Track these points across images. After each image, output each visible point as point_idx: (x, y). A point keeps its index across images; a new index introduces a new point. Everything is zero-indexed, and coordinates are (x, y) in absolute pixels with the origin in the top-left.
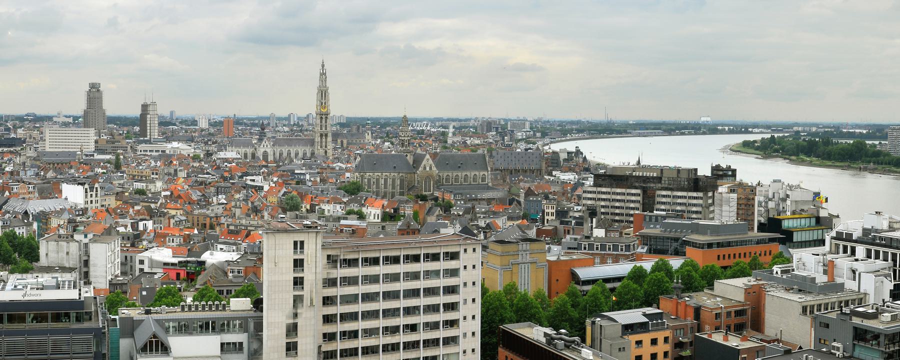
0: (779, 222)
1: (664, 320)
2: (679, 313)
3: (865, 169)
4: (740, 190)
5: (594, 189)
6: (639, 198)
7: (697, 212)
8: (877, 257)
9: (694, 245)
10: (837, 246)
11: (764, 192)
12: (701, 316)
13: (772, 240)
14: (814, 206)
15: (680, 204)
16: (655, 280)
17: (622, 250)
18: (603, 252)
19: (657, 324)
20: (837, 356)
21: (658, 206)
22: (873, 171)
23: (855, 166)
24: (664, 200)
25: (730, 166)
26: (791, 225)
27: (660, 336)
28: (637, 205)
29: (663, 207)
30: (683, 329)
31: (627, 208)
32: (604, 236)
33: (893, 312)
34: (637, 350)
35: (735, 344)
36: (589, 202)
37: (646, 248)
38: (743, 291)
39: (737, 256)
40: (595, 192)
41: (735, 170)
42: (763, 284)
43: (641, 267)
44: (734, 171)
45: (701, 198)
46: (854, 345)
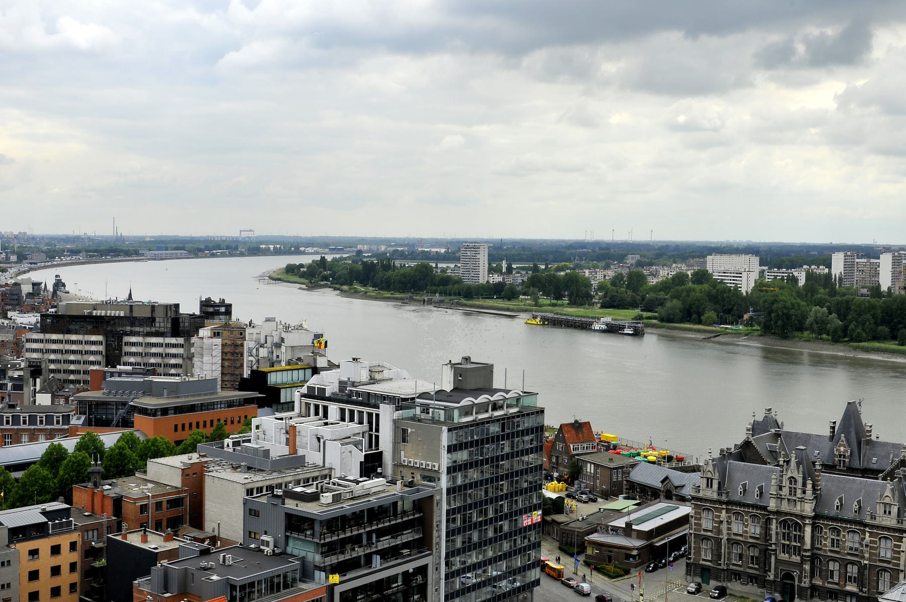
0: (264, 375)
1: (71, 519)
2: (96, 508)
3: (430, 302)
4: (226, 334)
5: (41, 336)
6: (101, 348)
7: (175, 366)
8: (352, 420)
9: (144, 411)
10: (308, 405)
11: (255, 336)
12: (123, 510)
13: (248, 401)
14: (313, 353)
15: (155, 355)
16: (74, 463)
17: (58, 422)
18: (33, 427)
19: (61, 525)
20: (265, 553)
21: (125, 359)
22: (439, 304)
23: (418, 298)
24: (133, 349)
25: (224, 300)
26: (279, 381)
27: (64, 541)
28: (99, 358)
29: (132, 360)
30: (97, 529)
31: (66, 362)
32: (50, 404)
33: (335, 491)
34: (31, 563)
35: (153, 546)
36: (35, 355)
37: (83, 417)
38: (180, 472)
39: (194, 425)
40: (41, 341)
41: (230, 305)
42: (206, 462)
43: (60, 445)
44: (229, 307)
45: (182, 346)
46: (287, 537)
